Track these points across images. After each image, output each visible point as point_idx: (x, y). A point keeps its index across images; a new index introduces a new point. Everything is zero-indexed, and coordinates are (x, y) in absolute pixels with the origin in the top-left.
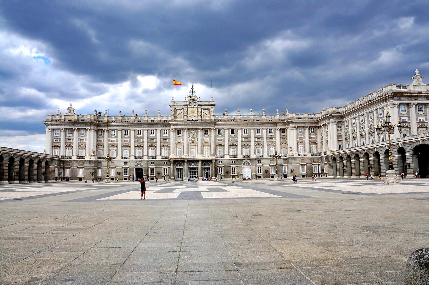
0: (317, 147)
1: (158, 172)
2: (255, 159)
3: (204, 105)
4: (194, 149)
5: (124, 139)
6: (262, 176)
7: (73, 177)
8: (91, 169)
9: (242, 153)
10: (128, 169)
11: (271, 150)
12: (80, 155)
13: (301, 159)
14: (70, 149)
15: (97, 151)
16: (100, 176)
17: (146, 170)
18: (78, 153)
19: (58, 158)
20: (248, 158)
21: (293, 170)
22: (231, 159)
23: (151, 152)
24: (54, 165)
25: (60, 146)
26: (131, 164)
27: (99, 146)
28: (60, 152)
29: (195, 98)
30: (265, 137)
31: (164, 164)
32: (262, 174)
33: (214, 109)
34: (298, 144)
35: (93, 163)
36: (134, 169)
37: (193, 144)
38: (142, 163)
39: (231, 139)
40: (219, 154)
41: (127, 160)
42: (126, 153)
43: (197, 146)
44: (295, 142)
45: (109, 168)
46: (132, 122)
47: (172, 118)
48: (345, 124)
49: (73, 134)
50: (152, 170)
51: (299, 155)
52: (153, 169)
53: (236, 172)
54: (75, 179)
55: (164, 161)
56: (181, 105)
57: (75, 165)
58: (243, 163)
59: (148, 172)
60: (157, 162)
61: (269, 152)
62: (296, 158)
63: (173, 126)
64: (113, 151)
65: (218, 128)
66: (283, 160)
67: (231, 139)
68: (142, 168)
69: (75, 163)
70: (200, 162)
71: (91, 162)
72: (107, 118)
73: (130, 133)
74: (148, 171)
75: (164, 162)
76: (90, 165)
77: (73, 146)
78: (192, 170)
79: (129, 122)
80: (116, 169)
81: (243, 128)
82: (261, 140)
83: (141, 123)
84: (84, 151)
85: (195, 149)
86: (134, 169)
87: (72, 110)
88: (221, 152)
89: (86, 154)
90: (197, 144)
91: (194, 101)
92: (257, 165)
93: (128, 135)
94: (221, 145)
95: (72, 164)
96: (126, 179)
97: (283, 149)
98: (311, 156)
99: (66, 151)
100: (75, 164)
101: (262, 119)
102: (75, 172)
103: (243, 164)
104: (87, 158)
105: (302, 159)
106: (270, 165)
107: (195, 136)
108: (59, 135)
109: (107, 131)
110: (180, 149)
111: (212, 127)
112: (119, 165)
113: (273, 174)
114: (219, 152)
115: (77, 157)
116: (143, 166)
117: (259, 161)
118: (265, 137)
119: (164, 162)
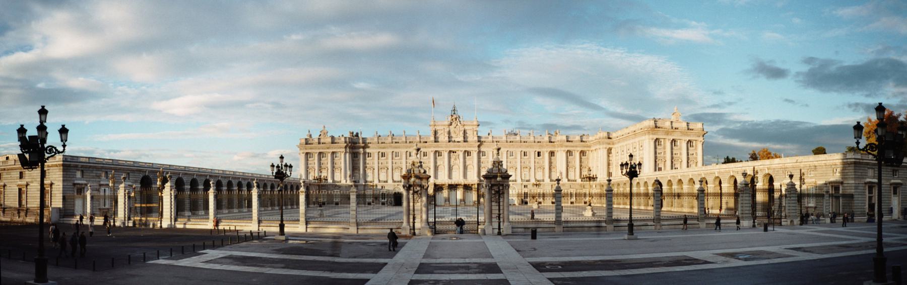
2: (522, 184)
3: (467, 125)
15: (353, 174)
20: (514, 182)
47: (432, 139)
49: (328, 156)
56: (442, 125)
62: (566, 183)
63: (434, 147)
73: (387, 155)
79: (387, 143)
83: (397, 144)
84: (339, 174)
89: (341, 178)
93: (385, 158)
96: (383, 204)
104: (343, 182)
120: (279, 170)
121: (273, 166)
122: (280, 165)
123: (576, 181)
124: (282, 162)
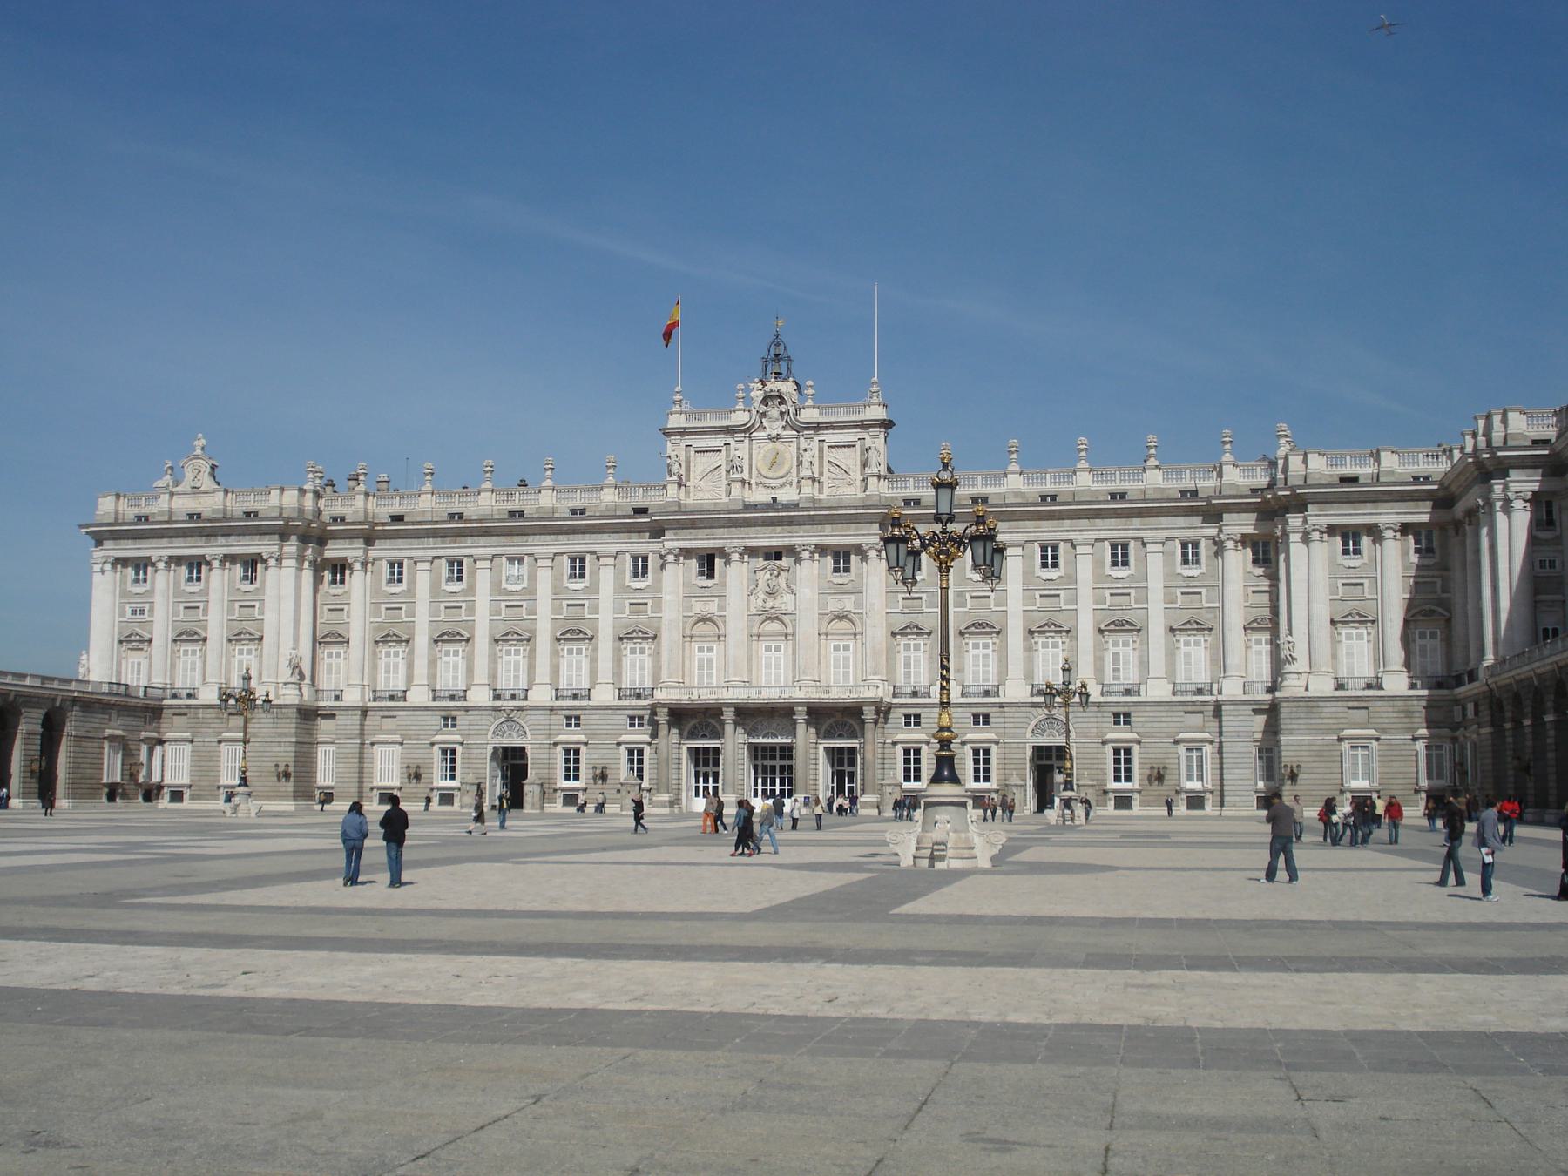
0: (1448, 641)
1: (598, 766)
3: (831, 426)
4: (778, 649)
5: (443, 605)
6: (1136, 796)
7: (202, 783)
8: (278, 749)
9: (1029, 676)
10: (459, 749)
13: (1351, 704)
14: (194, 652)
16: (327, 783)
17: (542, 756)
18: (228, 671)
19: (127, 695)
21: (1298, 767)
22: (970, 705)
23: (570, 666)
24: (97, 725)
25: (150, 641)
26: (471, 727)
27: (327, 639)
28: (150, 666)
29: (787, 388)
30: (1156, 584)
31: (632, 725)
32: (1134, 785)
34: (1333, 622)
35: (288, 721)
36: (484, 751)
37: (775, 626)
38: (524, 725)
39: (968, 596)
40: (907, 675)
41: (452, 704)
42: (451, 672)
43: (794, 634)
44: (1323, 612)
45: (372, 744)
46: (480, 521)
50: (572, 754)
51: (1340, 687)
52: (577, 752)
53: (993, 774)
54: (206, 793)
55: (631, 713)
57: (211, 730)
58: (1033, 723)
59: (551, 767)
60: (597, 717)
61: (1178, 667)
63: (676, 534)
64: (392, 659)
66: (1253, 710)
67: (968, 596)
68: (523, 749)
69: (210, 721)
70: (801, 716)
71: (280, 716)
72: (366, 504)
73: (473, 573)
74: (551, 761)
75: (632, 718)
76: (274, 730)
77: (205, 639)
78: (773, 758)
80: (405, 751)
81: (1032, 537)
82: (1133, 602)
85: (786, 652)
86: (484, 751)
87: (203, 470)
88: (917, 661)
90: (794, 627)
91: (780, 403)
92: (1110, 736)
94: (917, 628)
95: (198, 725)
97: (1255, 648)
98: (1410, 689)
99: (177, 660)
100: (212, 725)
101: (1141, 485)
102: (211, 764)
103: (1030, 730)
105: (1356, 704)
106: (1182, 736)
107: (783, 585)
108: (148, 588)
109: (364, 564)
110: (710, 650)
112: (417, 732)
113: (1195, 785)
114: (907, 665)
115: (220, 689)
116: (529, 737)
118: (1156, 584)
119: (632, 718)
123: (1380, 687)
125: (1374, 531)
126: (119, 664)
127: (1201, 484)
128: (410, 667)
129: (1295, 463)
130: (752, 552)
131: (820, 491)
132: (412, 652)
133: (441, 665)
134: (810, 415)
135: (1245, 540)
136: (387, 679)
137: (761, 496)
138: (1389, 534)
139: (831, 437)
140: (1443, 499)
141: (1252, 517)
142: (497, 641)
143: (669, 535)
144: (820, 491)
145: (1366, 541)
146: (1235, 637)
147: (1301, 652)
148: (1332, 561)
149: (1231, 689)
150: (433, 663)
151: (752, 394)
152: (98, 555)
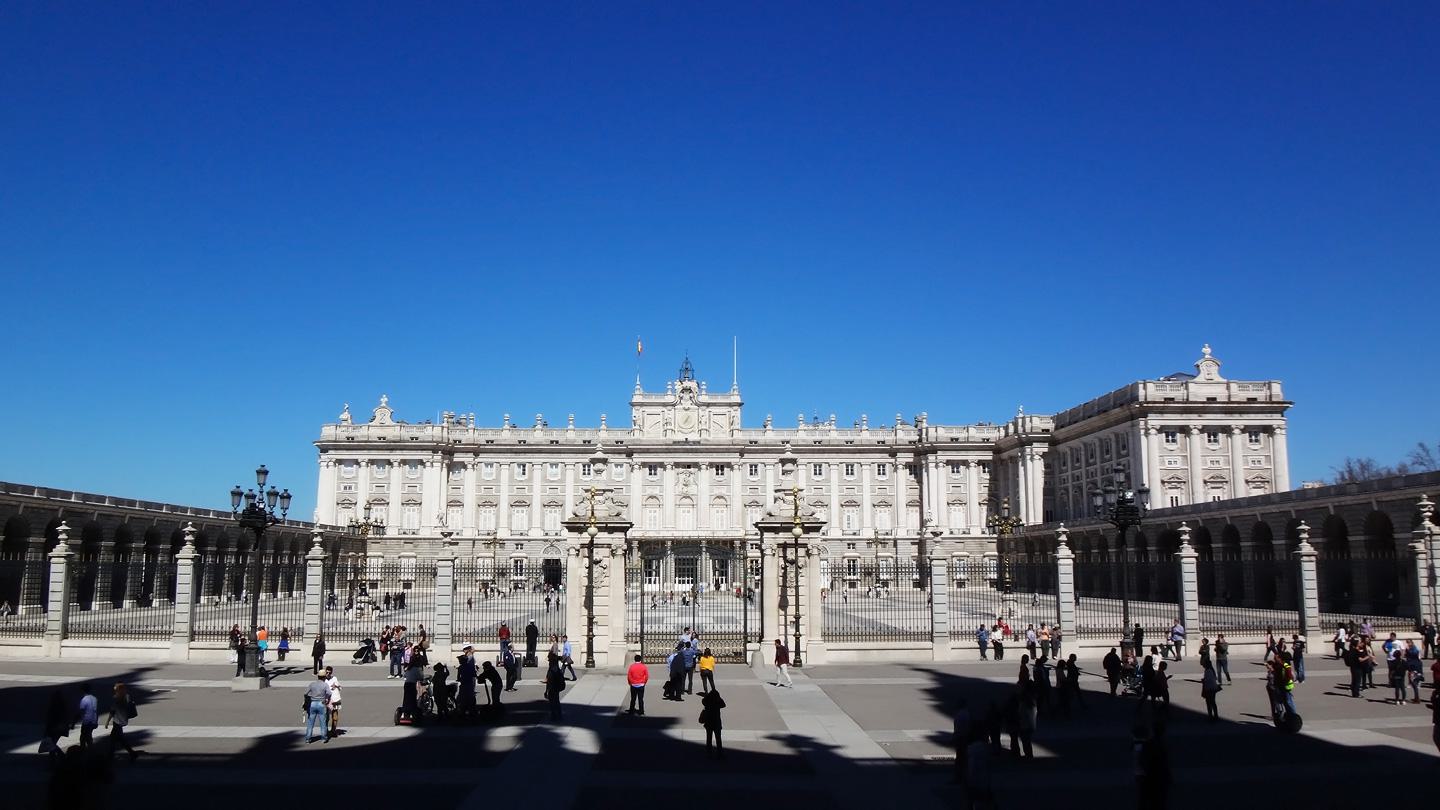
2: (841, 540)
3: (714, 404)
4: (689, 512)
11: (880, 517)
12: (405, 527)
18: (402, 520)
25: (356, 503)
32: (858, 577)
33: (738, 413)
34: (948, 504)
37: (688, 501)
48: (1059, 458)
51: (952, 533)
64: (488, 515)
65: (749, 459)
81: (810, 461)
92: (846, 555)
93: (526, 477)
97: (911, 514)
104: (424, 533)
110: (655, 512)
111: (734, 458)
117: (852, 545)
120: (253, 505)
121: (237, 494)
122: (256, 492)
124: (262, 485)
125: (966, 463)
126: (337, 516)
127: (887, 438)
128: (498, 517)
129: (932, 431)
130: (677, 465)
131: (709, 436)
132: (498, 511)
133: (514, 518)
134: (704, 399)
135: (908, 466)
136: (485, 525)
137: (681, 437)
138: (972, 464)
139: (712, 409)
140: (997, 450)
141: (912, 455)
142: (545, 506)
143: (635, 455)
144: (709, 436)
145: (962, 468)
146: (903, 509)
147: (934, 517)
148: (948, 477)
149: (901, 534)
150: (510, 516)
151: (676, 387)
152: (324, 457)
